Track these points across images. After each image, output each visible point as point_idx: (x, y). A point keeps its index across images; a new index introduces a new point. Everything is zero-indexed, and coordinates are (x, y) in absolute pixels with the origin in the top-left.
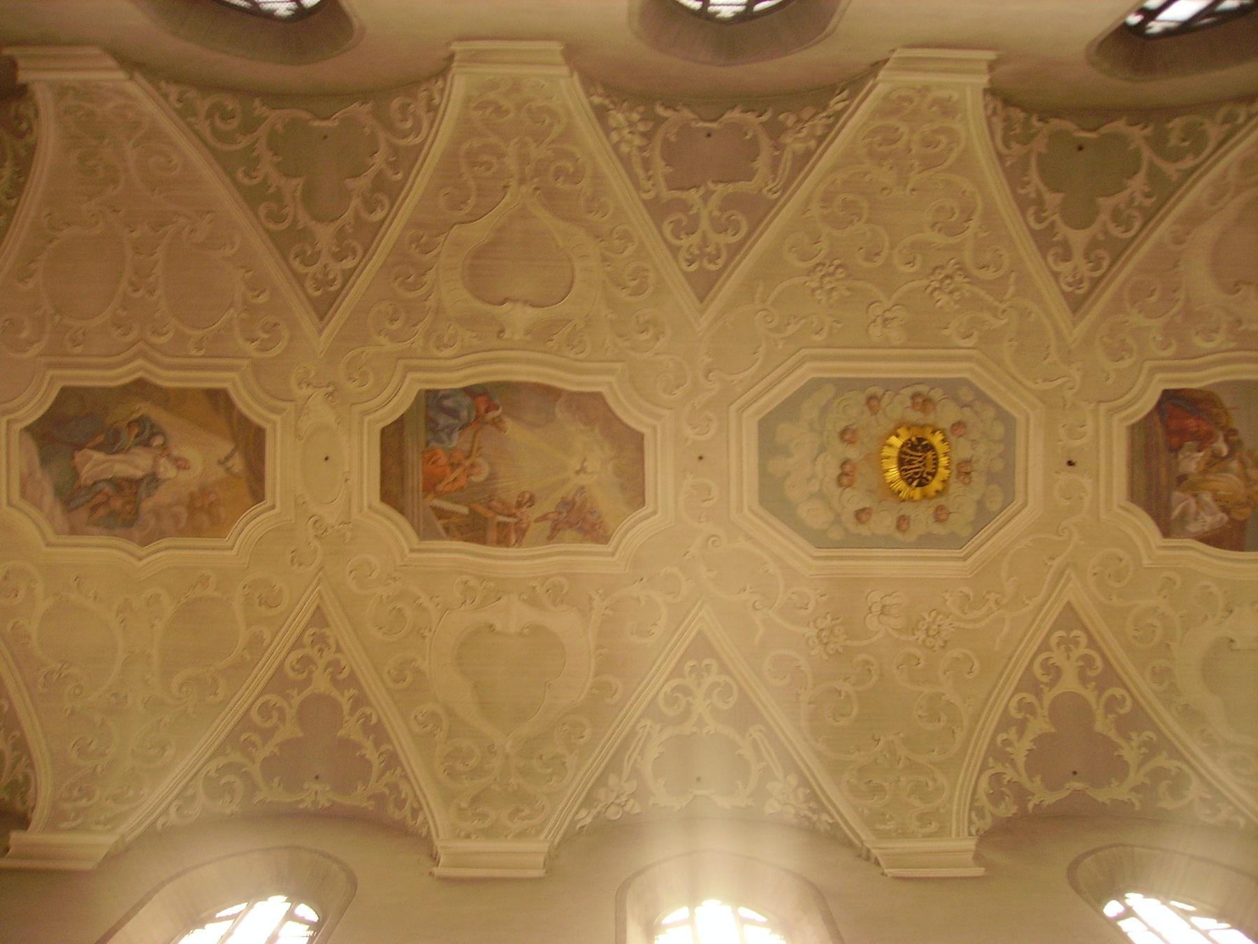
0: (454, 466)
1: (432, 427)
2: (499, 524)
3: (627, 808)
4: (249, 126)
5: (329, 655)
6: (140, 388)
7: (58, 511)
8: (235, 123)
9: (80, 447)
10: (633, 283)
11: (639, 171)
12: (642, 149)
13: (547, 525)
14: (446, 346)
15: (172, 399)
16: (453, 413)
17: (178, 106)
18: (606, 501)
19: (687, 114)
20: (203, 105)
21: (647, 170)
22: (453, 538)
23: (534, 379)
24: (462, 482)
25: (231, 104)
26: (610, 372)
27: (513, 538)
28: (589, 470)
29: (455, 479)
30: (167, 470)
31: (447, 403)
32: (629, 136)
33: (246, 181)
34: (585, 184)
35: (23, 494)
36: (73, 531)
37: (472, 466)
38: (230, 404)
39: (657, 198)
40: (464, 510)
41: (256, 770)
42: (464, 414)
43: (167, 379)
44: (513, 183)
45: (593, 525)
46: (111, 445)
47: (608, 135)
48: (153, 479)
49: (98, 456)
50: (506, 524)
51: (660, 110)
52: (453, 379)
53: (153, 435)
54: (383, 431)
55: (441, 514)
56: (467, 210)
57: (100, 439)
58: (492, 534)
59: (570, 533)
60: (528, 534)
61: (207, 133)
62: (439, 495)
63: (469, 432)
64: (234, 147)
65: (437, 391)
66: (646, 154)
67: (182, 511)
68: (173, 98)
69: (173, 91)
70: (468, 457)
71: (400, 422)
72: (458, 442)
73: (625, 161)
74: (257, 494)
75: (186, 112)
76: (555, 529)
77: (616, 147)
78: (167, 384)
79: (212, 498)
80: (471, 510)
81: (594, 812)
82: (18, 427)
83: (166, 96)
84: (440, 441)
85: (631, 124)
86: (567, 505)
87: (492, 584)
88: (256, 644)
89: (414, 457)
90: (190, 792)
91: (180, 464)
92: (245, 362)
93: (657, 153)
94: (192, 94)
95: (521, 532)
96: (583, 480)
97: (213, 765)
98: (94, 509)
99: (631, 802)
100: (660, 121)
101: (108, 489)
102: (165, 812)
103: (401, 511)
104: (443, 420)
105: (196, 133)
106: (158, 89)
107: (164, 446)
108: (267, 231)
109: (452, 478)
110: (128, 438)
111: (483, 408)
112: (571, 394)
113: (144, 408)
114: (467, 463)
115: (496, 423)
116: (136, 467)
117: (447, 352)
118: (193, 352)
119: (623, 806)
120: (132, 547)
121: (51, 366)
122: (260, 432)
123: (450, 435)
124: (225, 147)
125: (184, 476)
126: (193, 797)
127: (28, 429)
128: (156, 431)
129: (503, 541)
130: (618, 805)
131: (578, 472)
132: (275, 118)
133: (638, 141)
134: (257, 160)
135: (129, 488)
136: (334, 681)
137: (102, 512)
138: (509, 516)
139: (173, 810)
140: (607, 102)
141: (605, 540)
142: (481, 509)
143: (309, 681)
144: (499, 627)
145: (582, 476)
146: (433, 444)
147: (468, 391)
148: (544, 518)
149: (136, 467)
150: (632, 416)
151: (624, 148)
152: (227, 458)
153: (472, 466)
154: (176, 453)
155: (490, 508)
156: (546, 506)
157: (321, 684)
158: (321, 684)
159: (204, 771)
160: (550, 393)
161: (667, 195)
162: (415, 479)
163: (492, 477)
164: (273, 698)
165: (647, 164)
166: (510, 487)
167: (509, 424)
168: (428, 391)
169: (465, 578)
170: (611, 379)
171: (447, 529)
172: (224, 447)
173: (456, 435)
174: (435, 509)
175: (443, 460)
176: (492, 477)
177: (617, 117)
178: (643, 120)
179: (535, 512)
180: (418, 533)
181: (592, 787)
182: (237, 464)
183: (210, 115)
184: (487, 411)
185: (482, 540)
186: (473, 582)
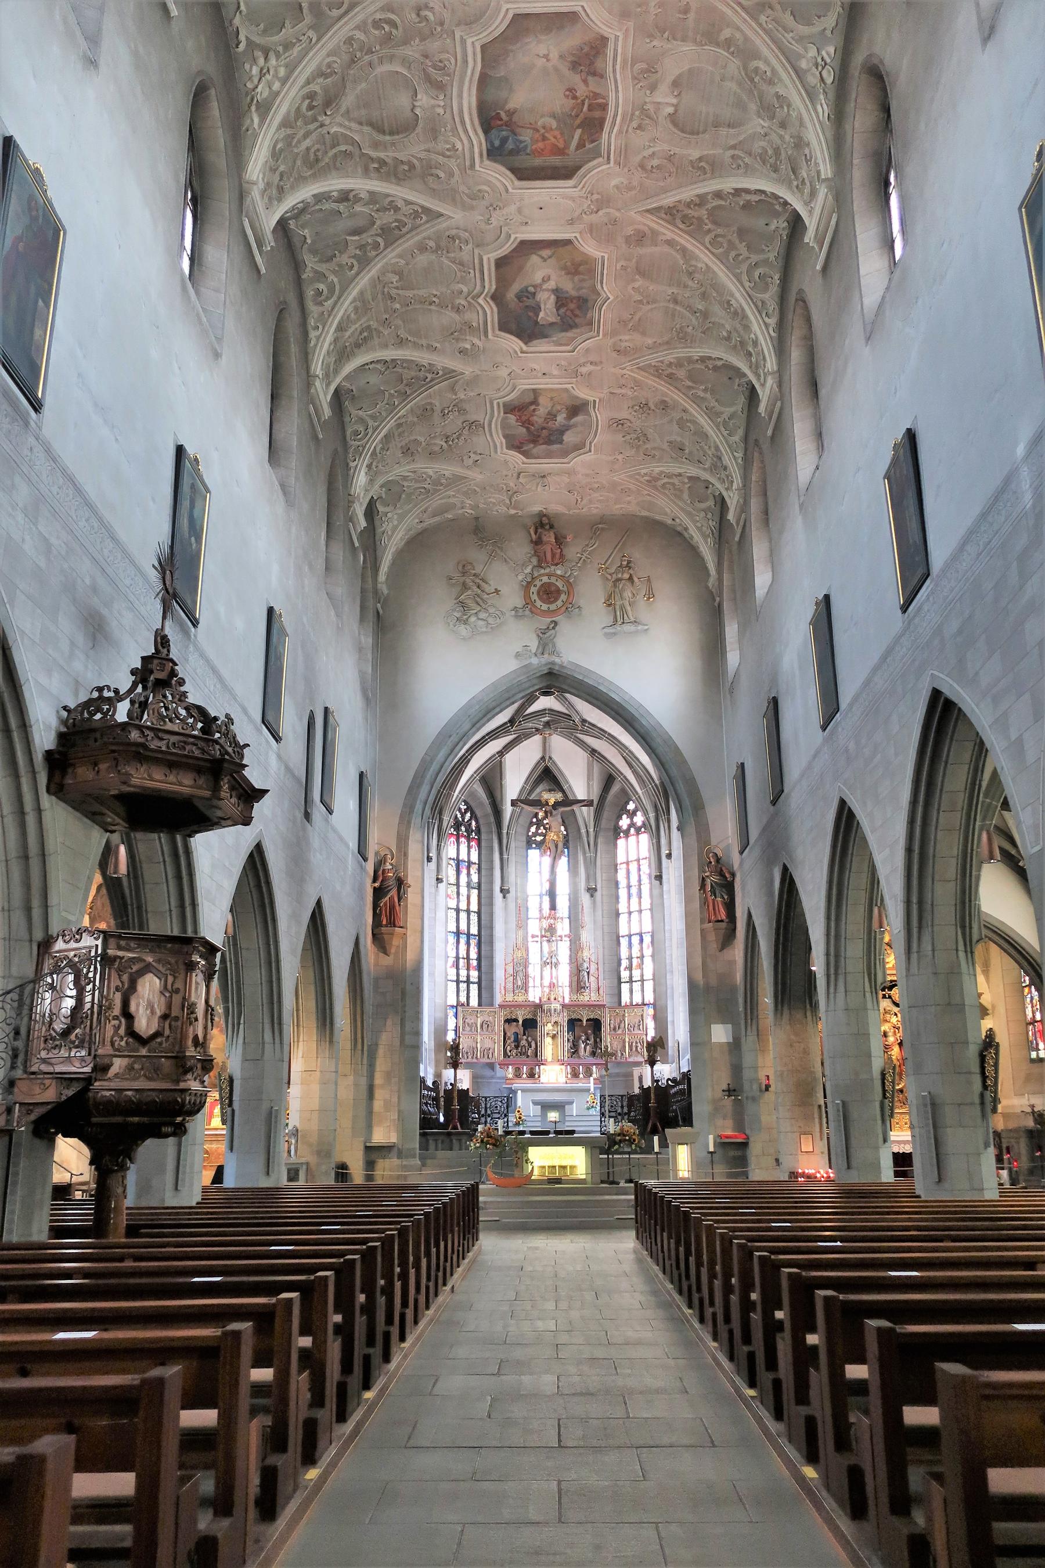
0: (544, 138)
1: (516, 152)
2: (589, 110)
3: (828, 61)
4: (321, 276)
5: (681, 207)
6: (497, 297)
7: (575, 331)
8: (321, 287)
9: (536, 323)
10: (387, 28)
11: (296, 50)
12: (278, 56)
13: (590, 78)
14: (454, 146)
15: (503, 282)
16: (504, 141)
17: (321, 327)
18: (572, 40)
19: (237, 21)
20: (313, 309)
21: (294, 44)
22: (600, 137)
23: (474, 91)
24: (557, 133)
25: (310, 293)
26: (463, 42)
27: (600, 101)
28: (546, 52)
29: (555, 137)
30: (552, 284)
31: (497, 143)
32: (271, 73)
33: (356, 268)
34: (315, 87)
35: (568, 345)
36: (590, 323)
37: (544, 128)
38: (505, 257)
39: (311, 27)
40: (579, 131)
41: (755, 258)
42: (504, 133)
43: (490, 286)
44: (324, 130)
45: (592, 47)
46: (537, 309)
47: (278, 93)
48: (556, 291)
49: (542, 315)
50: (589, 105)
51: (242, 47)
52: (478, 140)
53: (527, 291)
54: (520, 179)
55: (581, 145)
56: (349, 148)
57: (531, 314)
58: (597, 114)
59: (599, 64)
60: (598, 91)
61: (330, 302)
62: (567, 146)
63: (518, 130)
64: (336, 280)
65: (488, 150)
66: (280, 49)
67: (576, 278)
68: (317, 333)
69: (313, 334)
70: (538, 131)
71: (513, 170)
72: (526, 136)
73: (291, 68)
74: (569, 242)
75: (323, 319)
76: (594, 74)
77: (284, 81)
78: (494, 287)
79: (569, 264)
80: (578, 127)
81: (822, 97)
82: (525, 348)
83: (318, 338)
84: (526, 146)
85: (262, 75)
86: (575, 66)
87: (637, 113)
88: (670, 243)
89: (538, 162)
90: (760, 304)
91: (546, 279)
92: (476, 251)
93: (276, 38)
94: (312, 322)
95: (596, 95)
96: (554, 55)
97: (747, 284)
98: (576, 316)
99: (824, 53)
100: (250, 42)
101: (562, 311)
102: (766, 325)
103: (579, 168)
104: (510, 145)
105: (333, 308)
106: (316, 345)
107: (535, 286)
108: (385, 248)
109: (553, 140)
110: (530, 302)
111: (500, 123)
112: (483, 67)
113: (511, 295)
114: (542, 131)
115: (511, 113)
116: (549, 298)
117: (459, 146)
118: (472, 275)
119: (826, 64)
120: (599, 302)
121: (486, 336)
122: (523, 243)
123: (521, 142)
124: (337, 287)
125: (553, 277)
126: (763, 302)
127: (526, 343)
128: (525, 290)
129: (604, 107)
130: (823, 68)
131: (548, 60)
132: (311, 263)
133: (273, 62)
134: (340, 266)
135: (561, 300)
136: (700, 205)
137: (577, 312)
138: (583, 104)
139: (767, 320)
140: (253, 108)
141: (604, 40)
142: (578, 121)
143: (699, 219)
144: (670, 110)
145: (551, 56)
146: (528, 151)
147: (486, 132)
148: (585, 81)
149: (549, 298)
150: (498, 25)
151: (282, 72)
152: (542, 258)
153: (544, 128)
154: (539, 281)
155: (577, 116)
156: (576, 79)
157: (703, 213)
158: (703, 213)
159: (748, 289)
160: (484, 81)
161: (308, 19)
162: (556, 160)
163: (553, 116)
164: (707, 239)
165: (288, 46)
166: (560, 103)
167: (511, 105)
168: (488, 155)
169: (630, 130)
170: (469, 42)
171: (593, 141)
172: (534, 259)
173: (521, 138)
174: (578, 148)
175: (540, 145)
176: (553, 116)
177: (262, 92)
178: (255, 61)
179: (582, 91)
180: (594, 158)
181: (804, 86)
182: (545, 253)
183: (321, 304)
184: (501, 120)
185: (602, 122)
186: (635, 124)
